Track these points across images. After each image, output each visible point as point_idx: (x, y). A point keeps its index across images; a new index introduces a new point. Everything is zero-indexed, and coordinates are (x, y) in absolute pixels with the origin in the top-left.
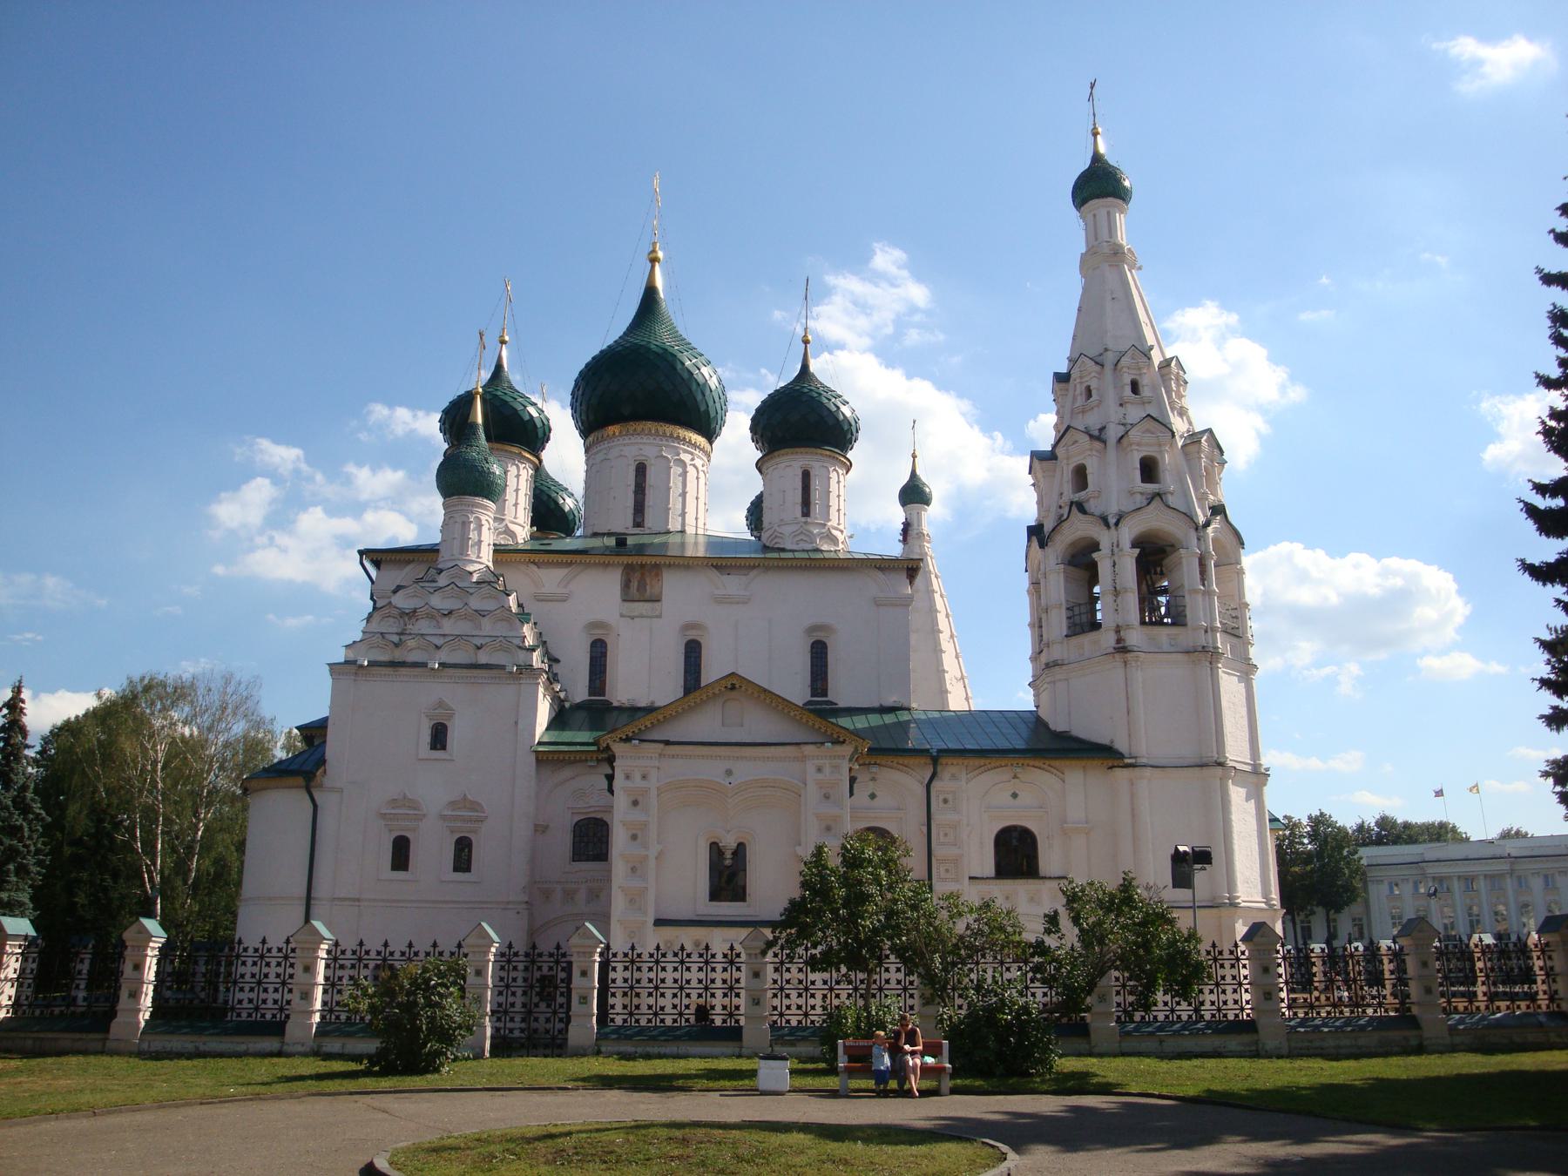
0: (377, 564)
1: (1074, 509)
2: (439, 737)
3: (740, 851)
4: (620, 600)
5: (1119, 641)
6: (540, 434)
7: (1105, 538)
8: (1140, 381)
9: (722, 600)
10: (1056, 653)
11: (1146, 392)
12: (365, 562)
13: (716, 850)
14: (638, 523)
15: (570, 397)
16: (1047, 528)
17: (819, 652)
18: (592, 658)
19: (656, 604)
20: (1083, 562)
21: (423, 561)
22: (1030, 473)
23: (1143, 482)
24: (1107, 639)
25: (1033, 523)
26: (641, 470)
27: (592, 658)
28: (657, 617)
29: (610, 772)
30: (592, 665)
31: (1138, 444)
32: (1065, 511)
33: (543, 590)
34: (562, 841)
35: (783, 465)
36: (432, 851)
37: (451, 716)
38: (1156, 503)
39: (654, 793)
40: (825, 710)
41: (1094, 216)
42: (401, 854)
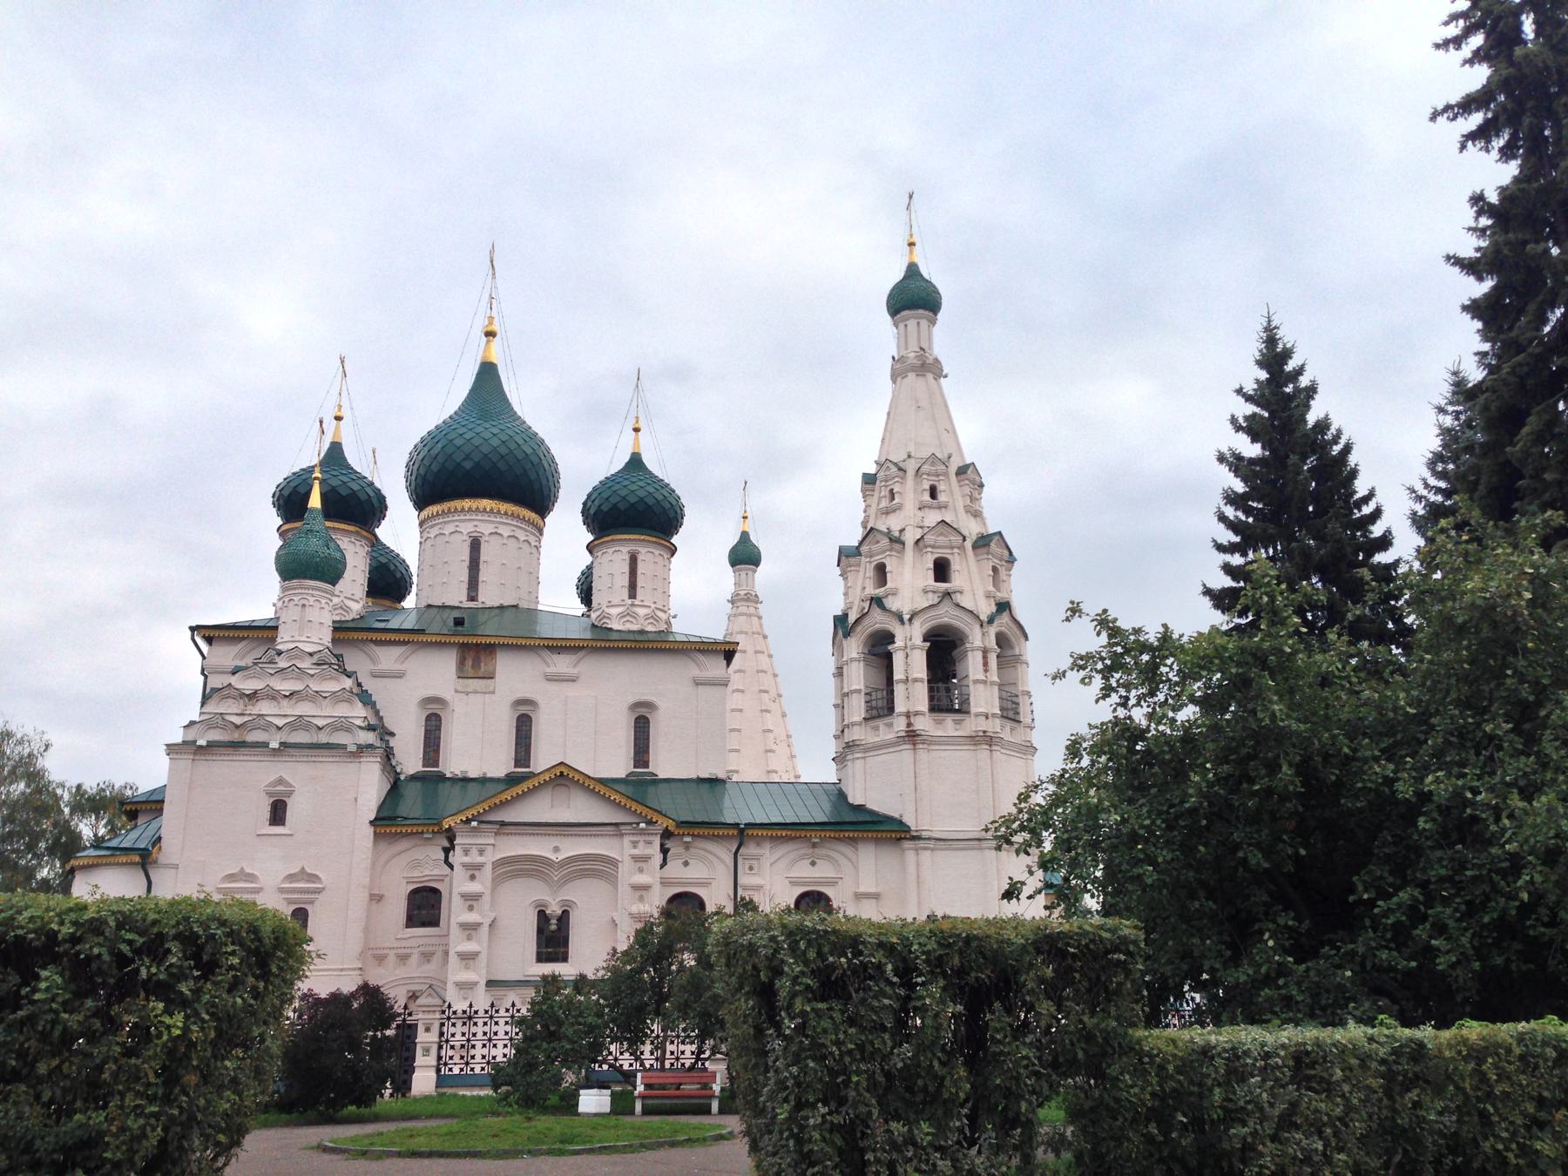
0: (209, 640)
1: (874, 606)
2: (278, 813)
3: (564, 918)
5: (909, 725)
6: (376, 504)
7: (900, 634)
9: (551, 679)
10: (856, 734)
11: (942, 498)
13: (543, 917)
14: (472, 598)
15: (405, 470)
16: (852, 618)
18: (427, 732)
20: (880, 649)
24: (900, 725)
25: (839, 613)
26: (475, 545)
27: (426, 731)
29: (447, 844)
30: (427, 738)
31: (933, 547)
32: (867, 605)
33: (380, 667)
34: (397, 908)
35: (610, 551)
37: (290, 794)
38: (947, 601)
39: (489, 868)
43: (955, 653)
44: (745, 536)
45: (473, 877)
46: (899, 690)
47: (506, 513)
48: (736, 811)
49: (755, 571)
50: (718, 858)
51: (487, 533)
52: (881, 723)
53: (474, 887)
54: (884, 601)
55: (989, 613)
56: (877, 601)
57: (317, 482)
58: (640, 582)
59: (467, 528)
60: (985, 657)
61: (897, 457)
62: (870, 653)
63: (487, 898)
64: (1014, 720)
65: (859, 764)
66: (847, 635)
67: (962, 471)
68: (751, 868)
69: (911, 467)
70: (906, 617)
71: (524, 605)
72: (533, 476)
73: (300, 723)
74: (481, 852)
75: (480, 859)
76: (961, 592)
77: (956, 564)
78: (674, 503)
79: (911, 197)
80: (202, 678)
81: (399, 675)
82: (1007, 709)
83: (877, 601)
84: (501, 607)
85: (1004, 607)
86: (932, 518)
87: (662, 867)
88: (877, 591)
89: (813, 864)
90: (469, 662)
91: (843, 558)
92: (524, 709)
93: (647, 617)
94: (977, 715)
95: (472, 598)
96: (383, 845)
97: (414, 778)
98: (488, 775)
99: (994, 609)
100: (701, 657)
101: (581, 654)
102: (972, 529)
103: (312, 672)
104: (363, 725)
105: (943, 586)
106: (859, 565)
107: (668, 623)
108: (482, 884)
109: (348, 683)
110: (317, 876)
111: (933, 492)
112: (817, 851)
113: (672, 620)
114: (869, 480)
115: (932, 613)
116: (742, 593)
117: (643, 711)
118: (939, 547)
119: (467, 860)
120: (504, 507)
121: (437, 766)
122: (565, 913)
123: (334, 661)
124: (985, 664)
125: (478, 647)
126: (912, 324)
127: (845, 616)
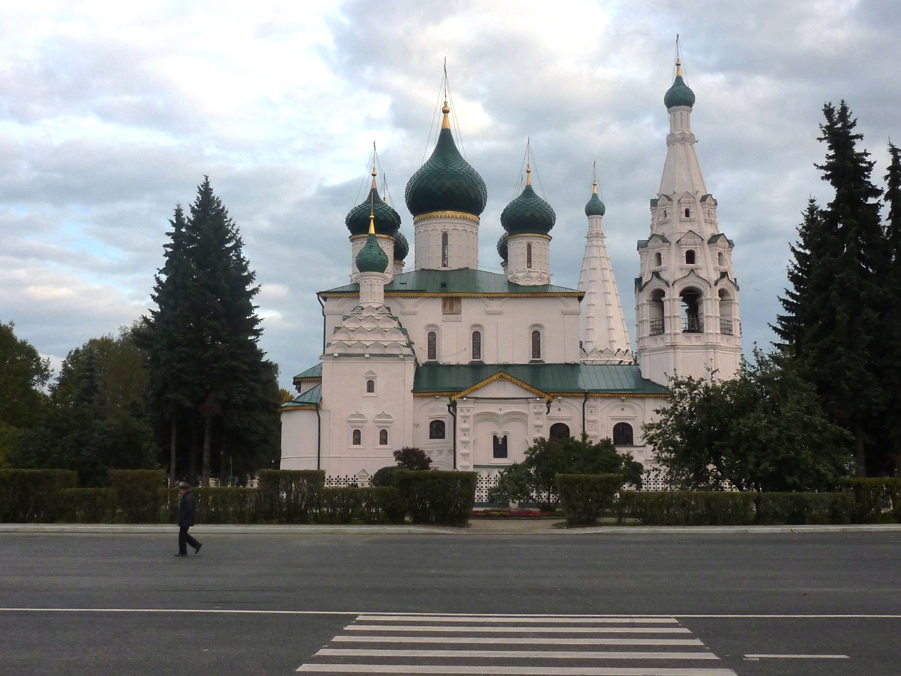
0: (325, 299)
1: (654, 276)
2: (371, 387)
4: (442, 314)
7: (667, 291)
8: (690, 209)
9: (489, 313)
11: (692, 216)
12: (320, 298)
17: (536, 338)
19: (458, 315)
21: (348, 297)
22: (638, 250)
23: (687, 263)
25: (639, 277)
26: (445, 236)
28: (459, 321)
31: (685, 245)
34: (426, 430)
36: (370, 437)
37: (375, 378)
38: (692, 274)
40: (538, 365)
41: (674, 114)
42: (357, 438)
43: (697, 300)
44: (595, 196)
45: (465, 421)
46: (667, 321)
47: (460, 218)
48: (586, 382)
49: (601, 218)
50: (573, 406)
51: (451, 229)
52: (658, 337)
53: (466, 426)
54: (660, 274)
55: (716, 279)
57: (372, 220)
58: (533, 259)
61: (669, 193)
62: (653, 300)
63: (471, 430)
64: (729, 335)
65: (647, 358)
66: (641, 290)
67: (704, 199)
68: (591, 412)
69: (675, 199)
70: (670, 284)
71: (471, 267)
72: (473, 196)
73: (377, 344)
74: (468, 411)
75: (468, 414)
76: (701, 269)
77: (698, 255)
78: (550, 214)
79: (678, 36)
80: (323, 317)
81: (414, 314)
82: (725, 329)
83: (656, 274)
84: (460, 270)
85: (724, 275)
86: (687, 227)
87: (547, 413)
88: (657, 268)
89: (623, 409)
90: (448, 305)
91: (640, 248)
92: (476, 329)
93: (537, 278)
96: (418, 401)
97: (425, 365)
98: (461, 363)
100: (564, 299)
101: (504, 300)
102: (708, 232)
103: (378, 318)
104: (405, 344)
105: (691, 265)
106: (648, 252)
107: (549, 279)
108: (470, 425)
109: (396, 324)
110: (389, 415)
111: (687, 213)
112: (626, 403)
113: (550, 277)
114: (654, 203)
116: (594, 232)
118: (689, 245)
119: (462, 414)
120: (459, 214)
121: (435, 359)
122: (505, 437)
123: (387, 312)
125: (452, 298)
126: (678, 113)
127: (641, 278)
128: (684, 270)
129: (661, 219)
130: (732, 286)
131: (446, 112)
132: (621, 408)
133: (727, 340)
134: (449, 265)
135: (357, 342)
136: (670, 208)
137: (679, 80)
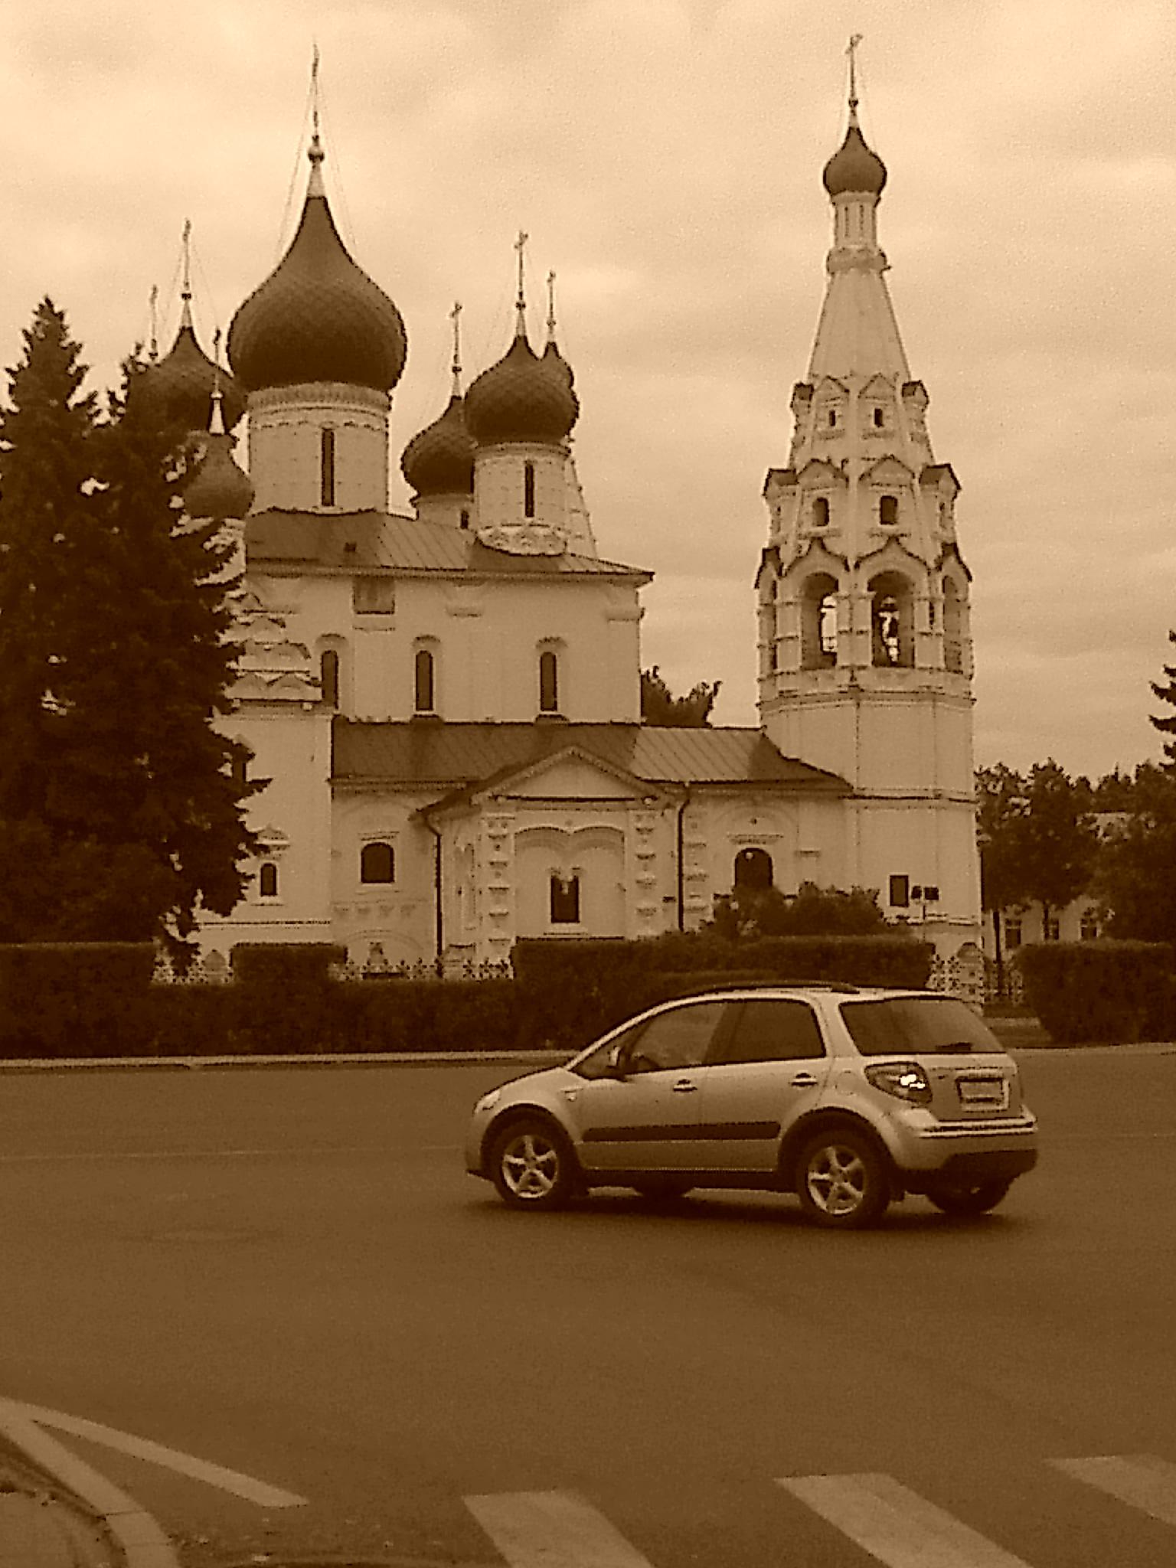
5: (852, 679)
13: (555, 883)
14: (328, 501)
17: (548, 665)
26: (328, 438)
53: (498, 856)
56: (819, 541)
59: (319, 418)
60: (931, 608)
62: (806, 595)
63: (510, 865)
64: (956, 672)
70: (851, 563)
75: (505, 831)
83: (819, 541)
85: (951, 549)
86: (879, 448)
88: (819, 529)
94: (921, 669)
95: (328, 501)
99: (940, 552)
105: (889, 528)
115: (879, 558)
117: (548, 648)
119: (492, 832)
122: (576, 881)
124: (932, 615)
127: (777, 549)
128: (876, 538)
129: (823, 426)
130: (964, 576)
131: (316, 158)
132: (751, 817)
133: (953, 681)
134: (336, 503)
135: (280, 674)
136: (842, 406)
137: (854, 132)
